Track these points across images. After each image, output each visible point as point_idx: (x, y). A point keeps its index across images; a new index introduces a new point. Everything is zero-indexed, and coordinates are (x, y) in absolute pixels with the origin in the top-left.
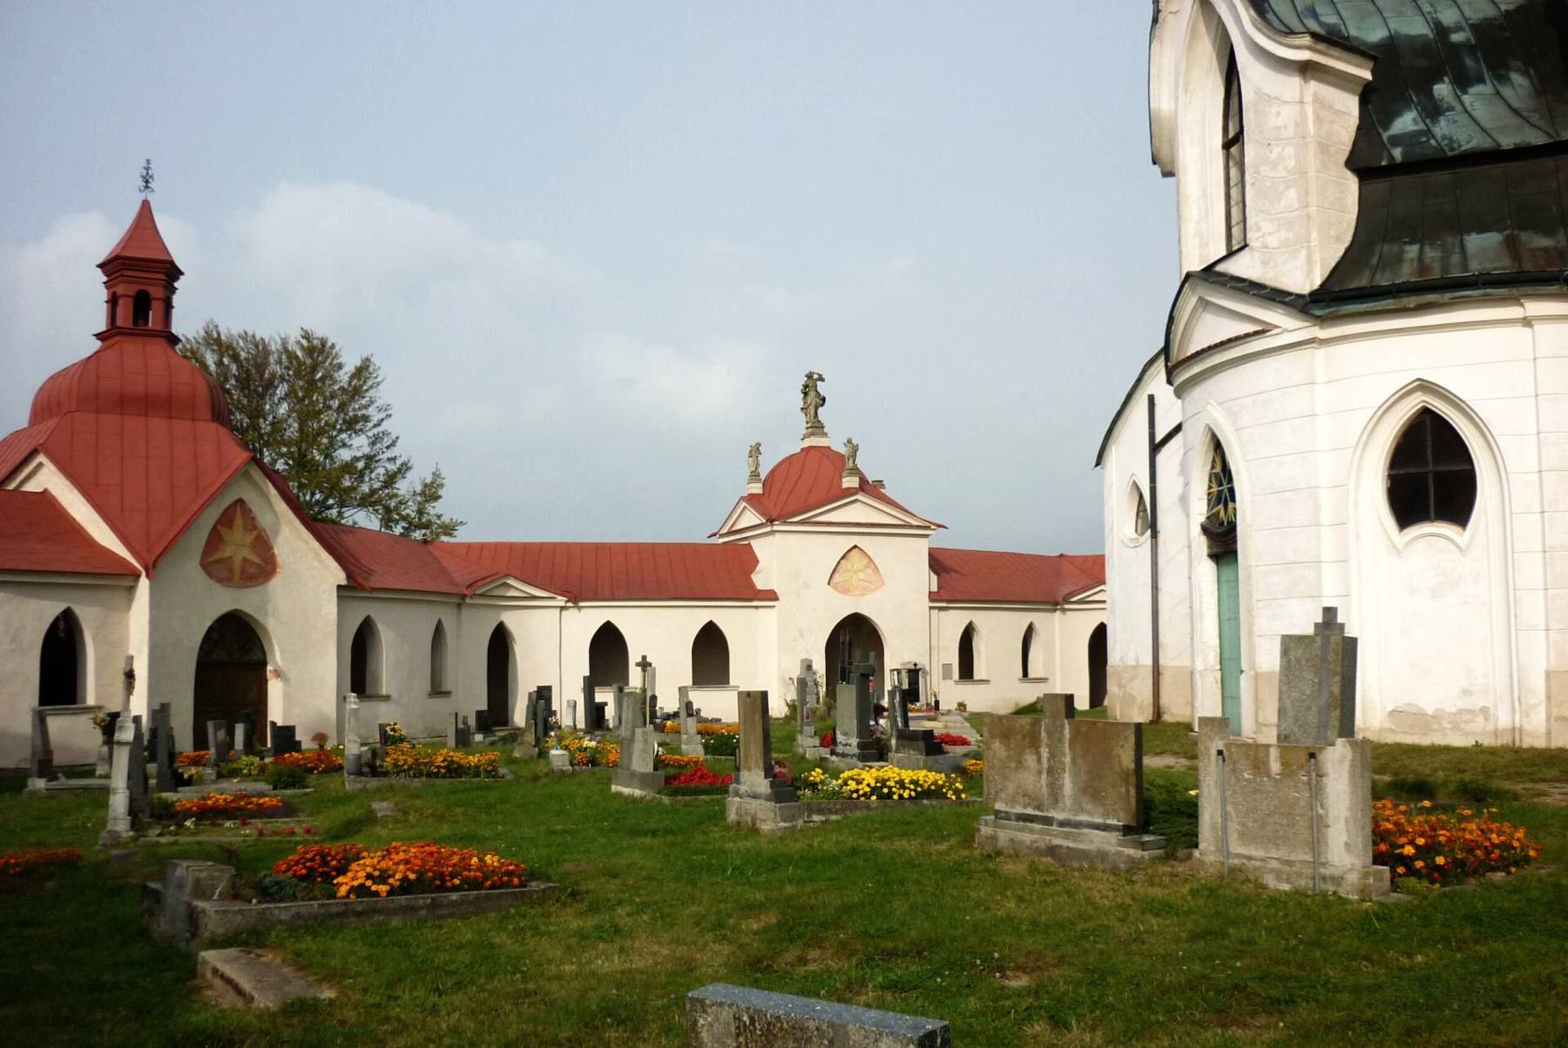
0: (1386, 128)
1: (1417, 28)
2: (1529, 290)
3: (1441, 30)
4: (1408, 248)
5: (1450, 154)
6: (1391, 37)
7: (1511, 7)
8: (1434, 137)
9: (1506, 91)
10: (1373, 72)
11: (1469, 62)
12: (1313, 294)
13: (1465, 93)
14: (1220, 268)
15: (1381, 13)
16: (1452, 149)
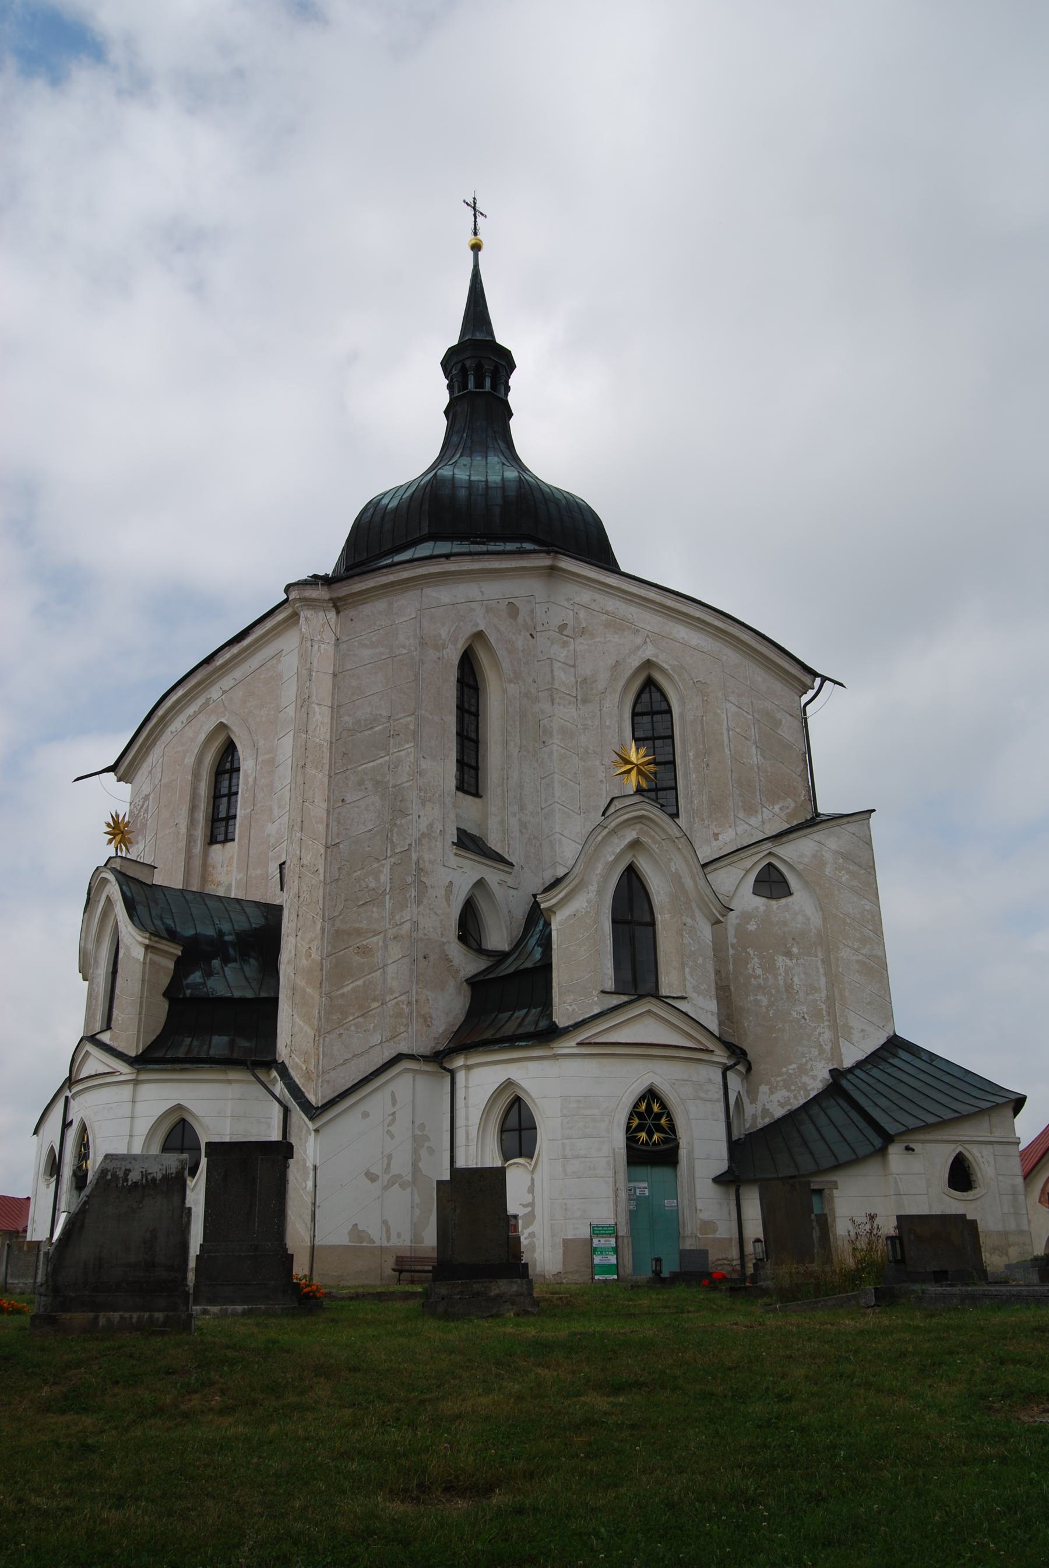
0: (186, 978)
1: (211, 932)
2: (230, 1066)
3: (221, 934)
4: (186, 1039)
5: (211, 996)
6: (196, 934)
7: (257, 926)
8: (206, 987)
9: (246, 968)
10: (182, 952)
11: (231, 951)
12: (137, 1057)
13: (226, 966)
14: (98, 1037)
15: (194, 921)
16: (212, 994)
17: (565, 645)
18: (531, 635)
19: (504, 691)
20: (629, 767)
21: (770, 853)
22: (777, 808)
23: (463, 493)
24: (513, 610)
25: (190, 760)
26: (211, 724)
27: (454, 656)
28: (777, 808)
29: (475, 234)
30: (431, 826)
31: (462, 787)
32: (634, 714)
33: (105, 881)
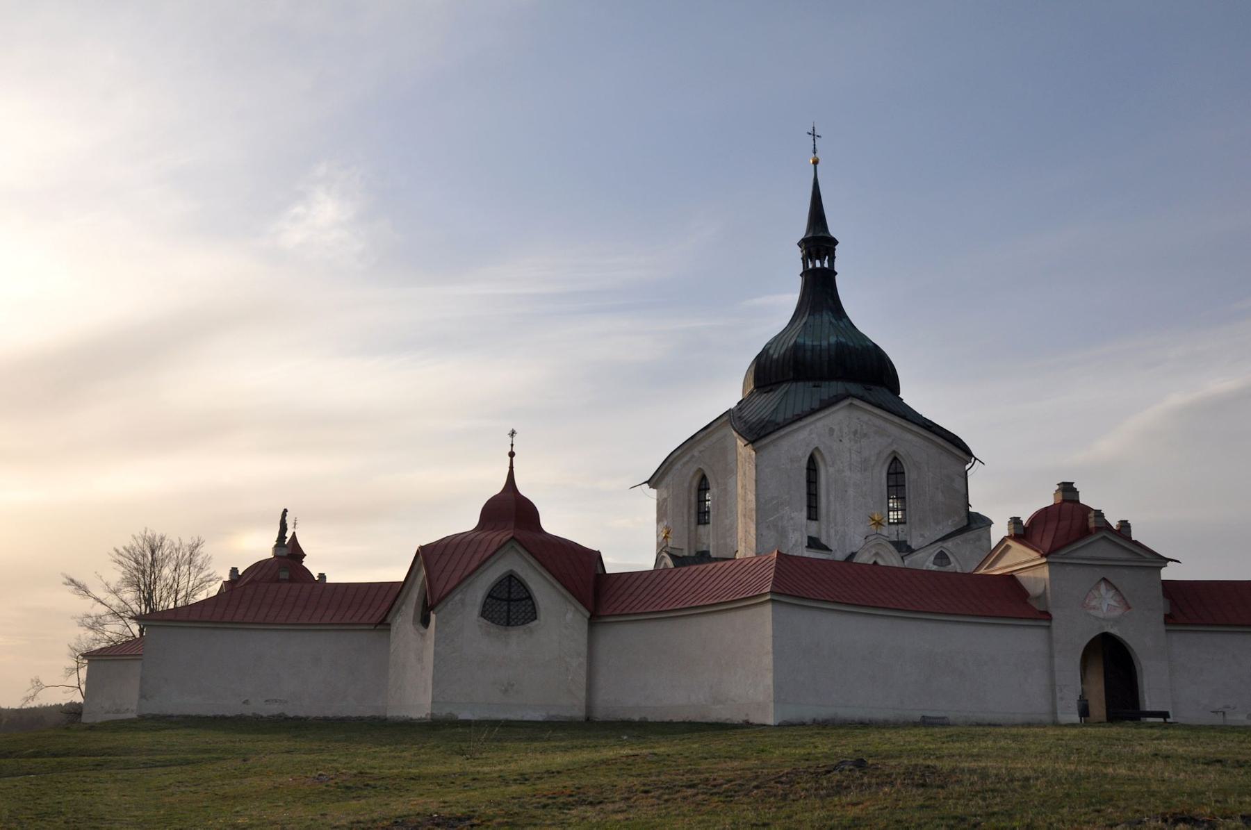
17: (856, 442)
18: (841, 441)
19: (827, 471)
20: (874, 522)
21: (941, 547)
22: (950, 521)
23: (809, 354)
24: (831, 430)
25: (686, 485)
26: (694, 469)
27: (804, 462)
28: (950, 521)
29: (815, 153)
30: (796, 541)
31: (810, 518)
32: (889, 474)
33: (664, 557)
